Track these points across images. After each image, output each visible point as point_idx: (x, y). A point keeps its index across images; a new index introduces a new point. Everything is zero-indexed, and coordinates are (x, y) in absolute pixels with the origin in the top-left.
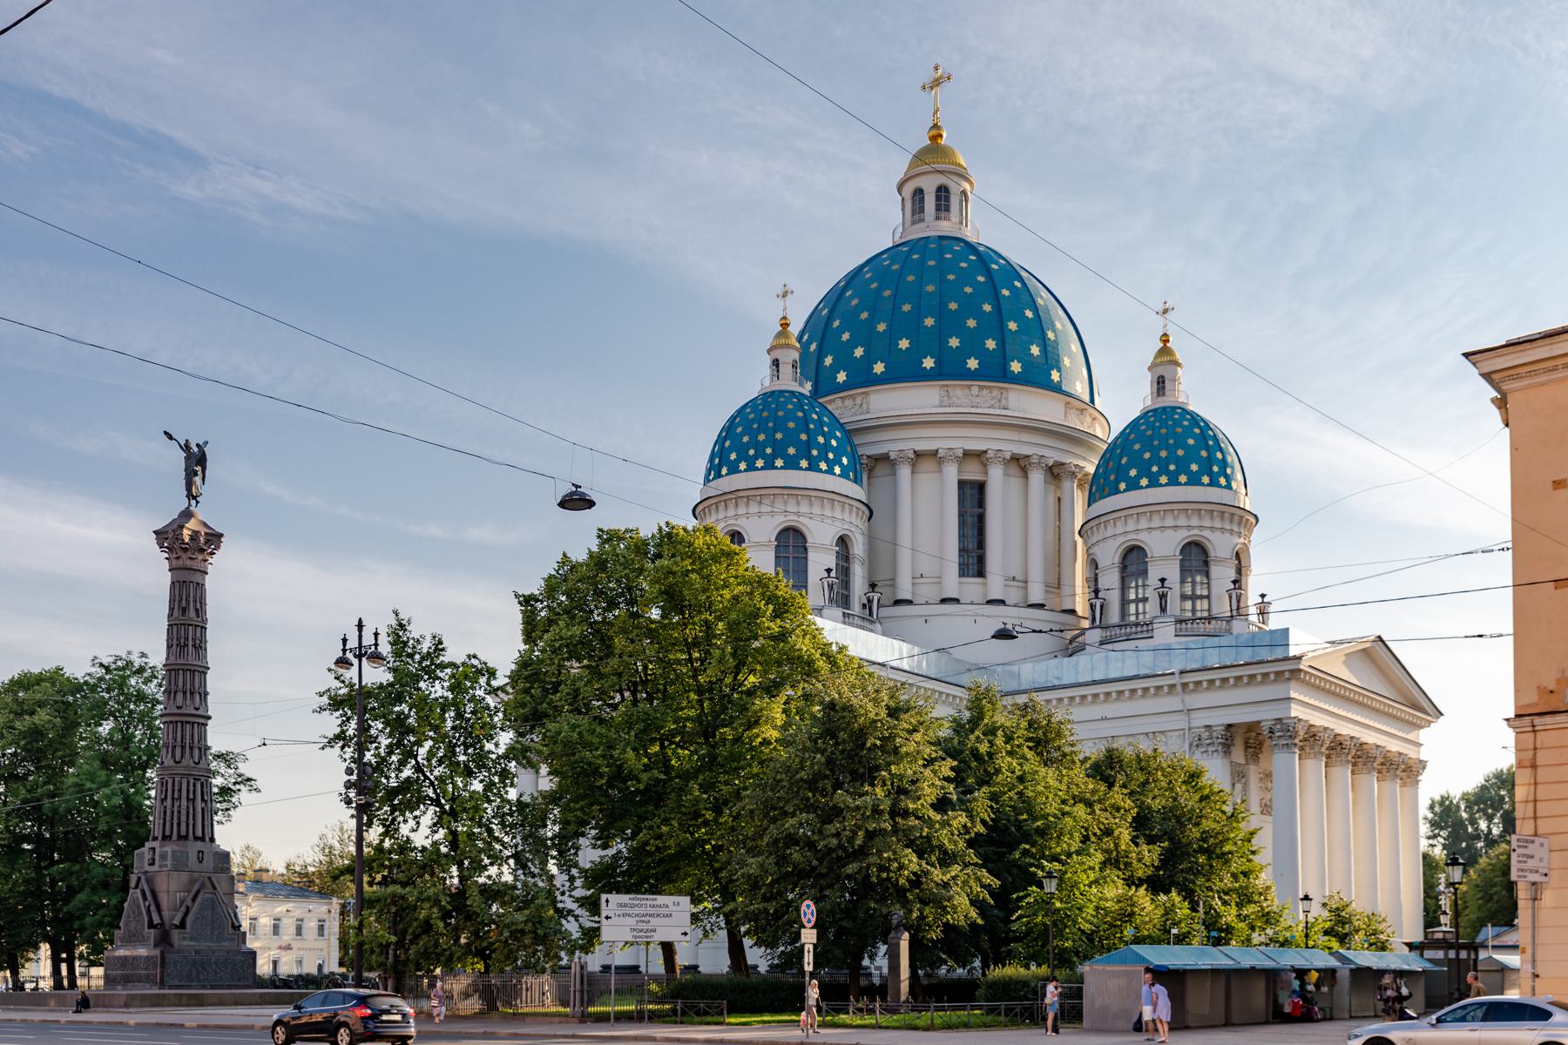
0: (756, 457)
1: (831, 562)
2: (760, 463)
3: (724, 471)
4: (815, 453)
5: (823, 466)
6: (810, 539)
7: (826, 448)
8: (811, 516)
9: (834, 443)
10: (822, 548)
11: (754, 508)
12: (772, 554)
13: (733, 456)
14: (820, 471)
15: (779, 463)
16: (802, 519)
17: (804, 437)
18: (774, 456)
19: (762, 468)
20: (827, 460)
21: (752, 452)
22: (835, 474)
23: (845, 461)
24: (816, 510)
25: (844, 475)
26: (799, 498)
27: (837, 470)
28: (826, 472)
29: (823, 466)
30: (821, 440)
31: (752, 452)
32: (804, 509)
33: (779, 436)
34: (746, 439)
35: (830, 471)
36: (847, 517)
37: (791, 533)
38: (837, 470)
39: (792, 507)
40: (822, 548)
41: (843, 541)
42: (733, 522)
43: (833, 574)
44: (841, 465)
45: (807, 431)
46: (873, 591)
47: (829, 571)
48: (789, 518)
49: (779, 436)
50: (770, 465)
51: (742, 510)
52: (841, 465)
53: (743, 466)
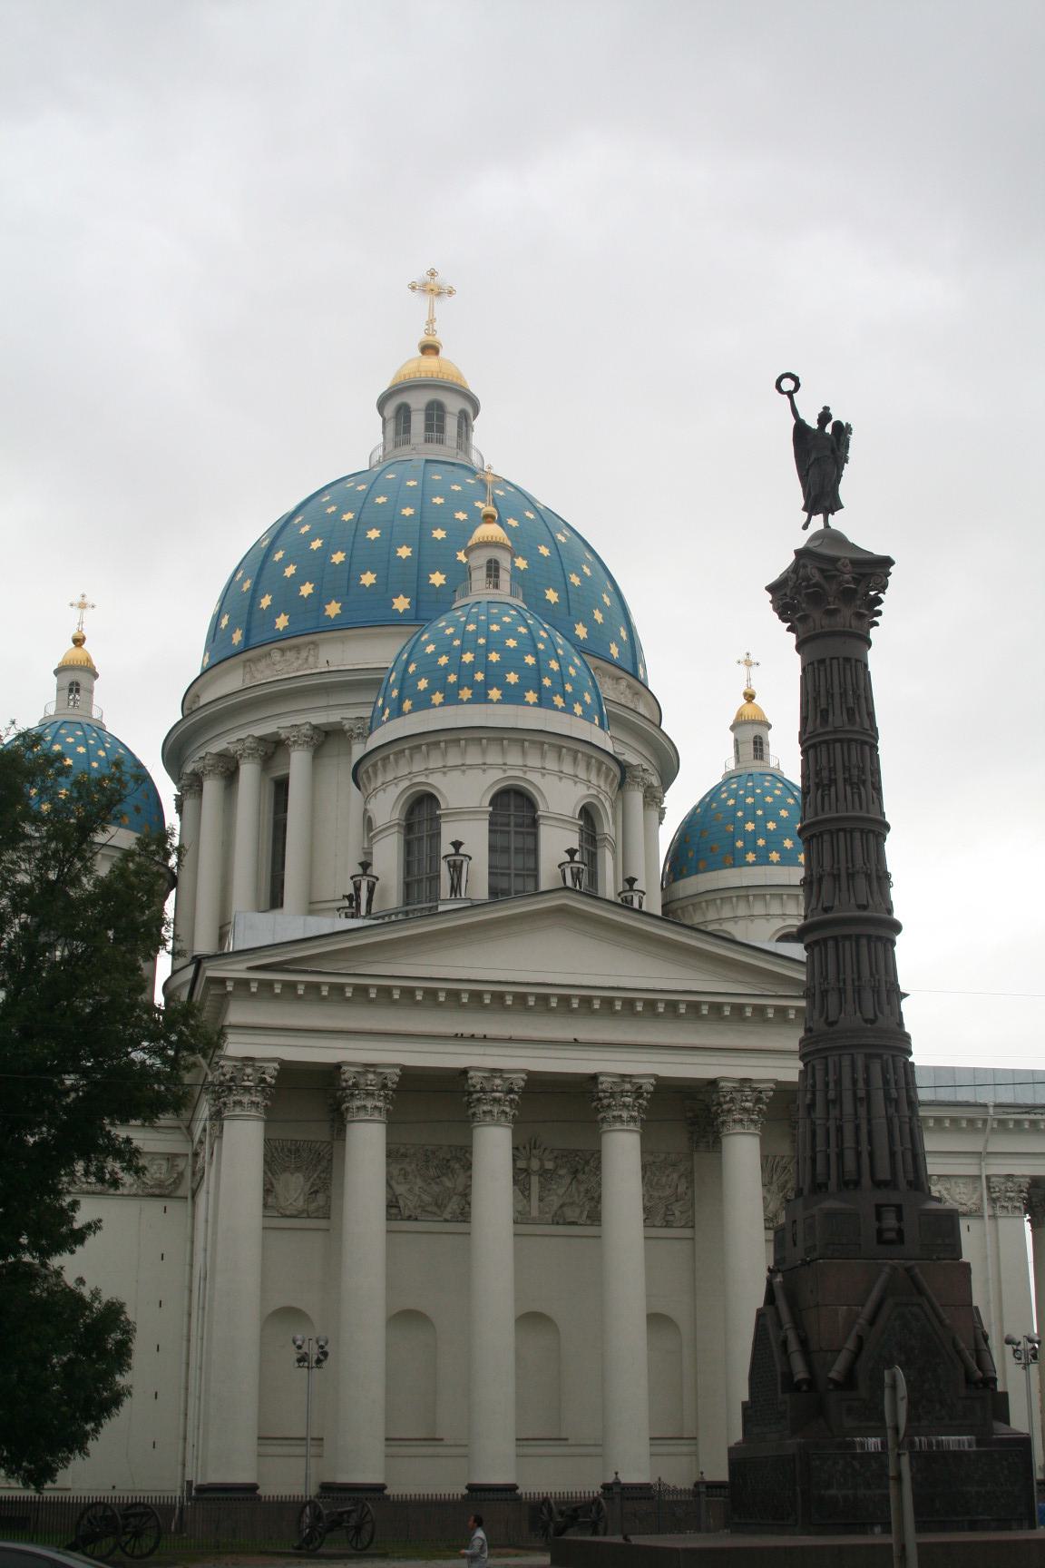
1: (573, 840)
2: (466, 694)
3: (407, 705)
4: (547, 682)
5: (558, 701)
6: (541, 806)
7: (561, 677)
8: (543, 771)
9: (572, 671)
10: (560, 820)
11: (454, 758)
12: (485, 825)
13: (423, 684)
14: (555, 708)
15: (495, 694)
16: (531, 776)
17: (530, 660)
18: (487, 685)
19: (469, 702)
20: (564, 695)
21: (452, 678)
22: (575, 714)
23: (587, 698)
24: (551, 764)
25: (587, 716)
27: (578, 709)
28: (563, 710)
29: (558, 701)
30: (554, 665)
32: (534, 761)
33: (494, 657)
34: (443, 660)
35: (568, 710)
37: (512, 794)
38: (578, 709)
39: (514, 758)
40: (560, 820)
41: (588, 814)
43: (577, 858)
44: (583, 703)
46: (631, 889)
47: (571, 852)
48: (510, 773)
49: (494, 657)
50: (481, 697)
51: (436, 761)
52: (583, 703)
53: (438, 698)
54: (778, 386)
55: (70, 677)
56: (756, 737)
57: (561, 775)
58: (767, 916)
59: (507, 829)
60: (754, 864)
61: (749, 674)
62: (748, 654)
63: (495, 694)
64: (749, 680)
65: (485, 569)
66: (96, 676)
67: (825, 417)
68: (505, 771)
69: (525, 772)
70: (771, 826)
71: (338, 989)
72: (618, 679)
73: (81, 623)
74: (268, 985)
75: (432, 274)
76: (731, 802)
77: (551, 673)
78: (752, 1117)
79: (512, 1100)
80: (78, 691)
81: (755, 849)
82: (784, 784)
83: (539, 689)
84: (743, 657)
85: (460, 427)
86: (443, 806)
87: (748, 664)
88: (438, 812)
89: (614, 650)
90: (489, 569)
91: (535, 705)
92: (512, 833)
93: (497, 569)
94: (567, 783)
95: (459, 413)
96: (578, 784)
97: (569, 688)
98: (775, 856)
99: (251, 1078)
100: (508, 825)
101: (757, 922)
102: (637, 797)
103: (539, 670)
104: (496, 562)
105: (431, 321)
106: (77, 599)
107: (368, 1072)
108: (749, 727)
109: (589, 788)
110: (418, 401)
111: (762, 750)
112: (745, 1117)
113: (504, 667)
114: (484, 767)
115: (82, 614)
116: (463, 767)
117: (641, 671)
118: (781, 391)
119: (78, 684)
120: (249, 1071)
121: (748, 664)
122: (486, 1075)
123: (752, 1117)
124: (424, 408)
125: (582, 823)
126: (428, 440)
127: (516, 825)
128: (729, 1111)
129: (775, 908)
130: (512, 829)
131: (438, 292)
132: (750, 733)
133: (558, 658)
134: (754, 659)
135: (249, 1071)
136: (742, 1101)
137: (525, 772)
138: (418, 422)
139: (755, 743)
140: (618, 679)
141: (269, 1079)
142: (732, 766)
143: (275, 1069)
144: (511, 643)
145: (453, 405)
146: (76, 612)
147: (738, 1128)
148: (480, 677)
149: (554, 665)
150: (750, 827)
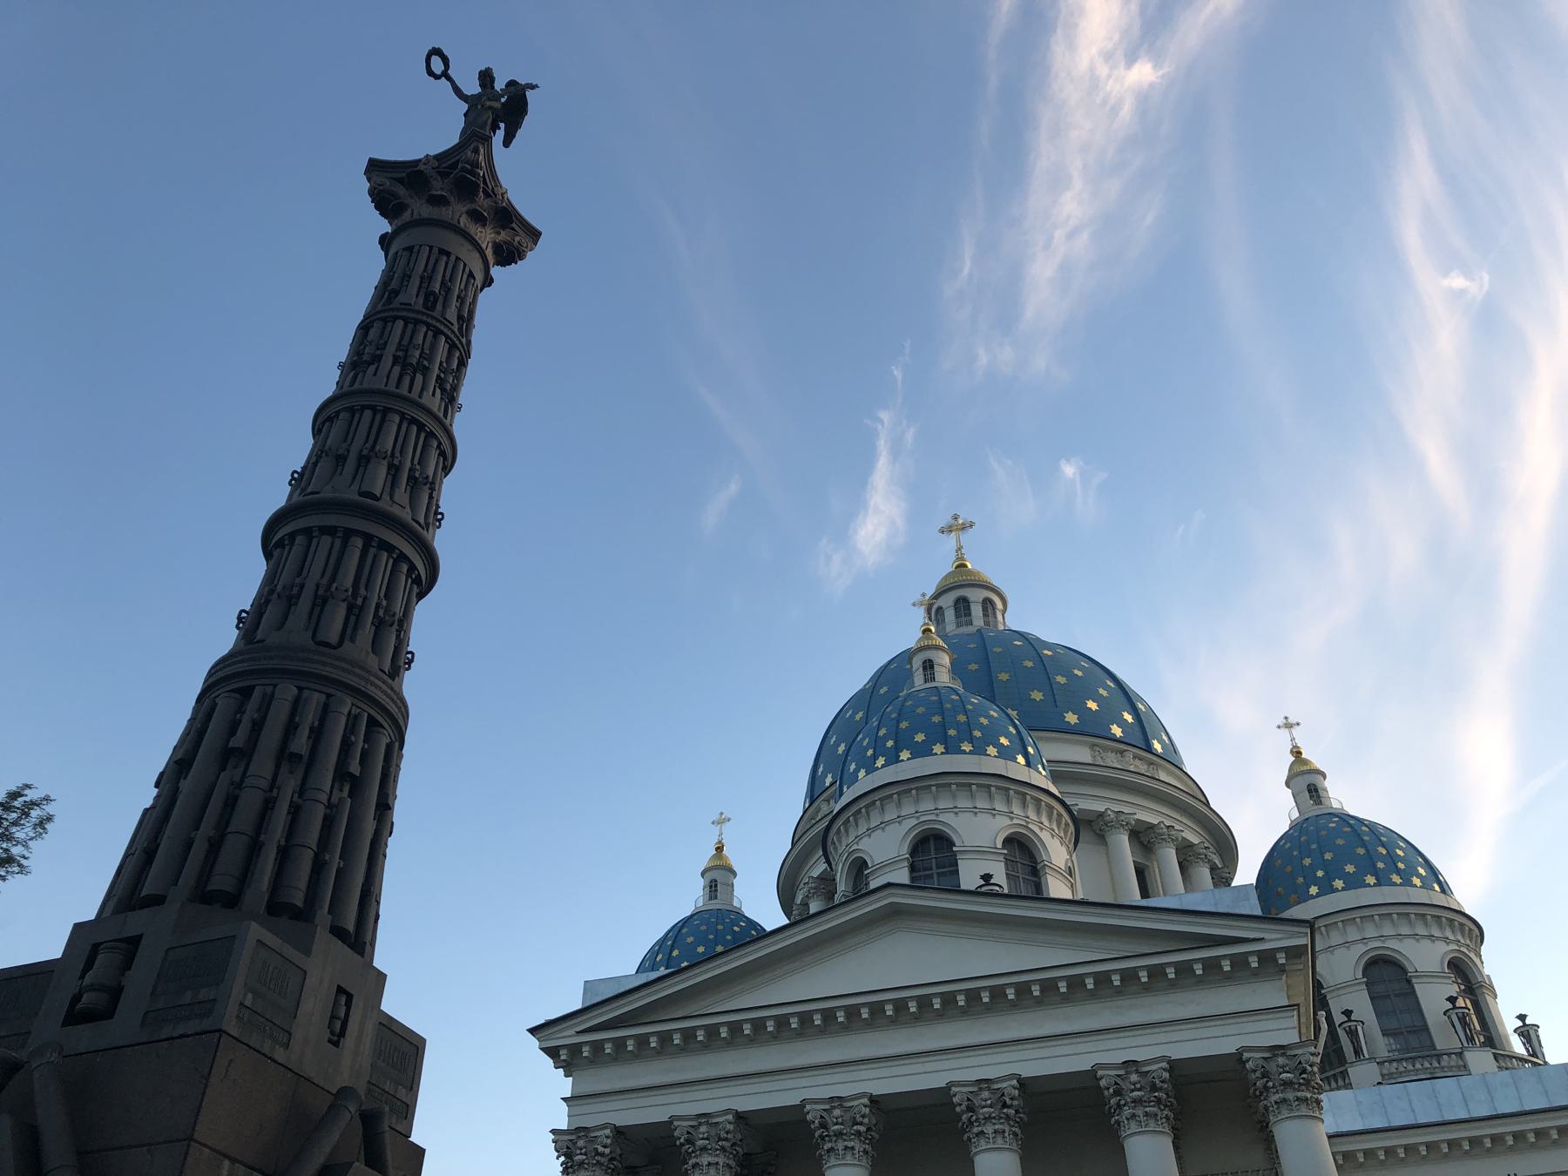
0: (875, 757)
2: (880, 762)
4: (952, 732)
5: (967, 747)
8: (956, 811)
10: (979, 852)
13: (853, 766)
14: (964, 752)
18: (897, 750)
20: (971, 740)
24: (963, 803)
26: (934, 788)
27: (992, 750)
28: (971, 753)
30: (962, 718)
31: (870, 752)
32: (943, 804)
33: (904, 725)
36: (1017, 810)
39: (926, 805)
40: (979, 852)
42: (855, 847)
45: (942, 713)
48: (922, 819)
51: (862, 829)
54: (430, 73)
55: (710, 875)
56: (1309, 786)
57: (975, 811)
58: (1347, 944)
59: (929, 872)
60: (1318, 895)
61: (1291, 733)
62: (1286, 718)
63: (905, 755)
64: (1293, 739)
65: (921, 669)
66: (734, 874)
67: (486, 77)
68: (918, 818)
69: (937, 815)
70: (1328, 856)
71: (665, 1038)
72: (1122, 752)
73: (721, 834)
74: (597, 1047)
75: (956, 518)
76: (1288, 845)
77: (958, 726)
78: (1148, 1109)
79: (859, 1133)
80: (716, 886)
81: (1317, 881)
82: (1339, 817)
83: (945, 740)
84: (1281, 721)
85: (985, 610)
86: (870, 866)
87: (1289, 726)
88: (866, 872)
89: (1117, 731)
90: (925, 669)
91: (942, 753)
92: (935, 876)
93: (932, 667)
94: (984, 818)
95: (983, 601)
96: (997, 816)
97: (977, 734)
98: (1339, 884)
99: (583, 1151)
100: (931, 869)
101: (1338, 952)
102: (1170, 855)
103: (944, 726)
104: (930, 661)
105: (959, 549)
106: (716, 817)
107: (700, 1124)
108: (1300, 778)
109: (1012, 819)
110: (947, 601)
111: (1319, 797)
112: (1139, 1112)
113: (914, 730)
114: (900, 819)
115: (721, 828)
116: (883, 825)
117: (1157, 746)
118: (437, 77)
119: (716, 881)
120: (581, 1143)
121: (1289, 726)
122: (827, 1107)
123: (1148, 1109)
124: (953, 604)
125: (1006, 852)
126: (959, 625)
127: (937, 868)
128: (1119, 1106)
129: (1353, 934)
130: (935, 871)
131: (964, 528)
132: (1302, 782)
133: (965, 712)
134: (1292, 720)
135: (581, 1143)
136: (1133, 1091)
137: (937, 815)
138: (950, 615)
139: (1310, 791)
140: (1122, 752)
141: (601, 1149)
142: (1296, 814)
143: (607, 1137)
144: (920, 710)
145: (976, 596)
146: (716, 829)
147: (1134, 1127)
148: (890, 744)
149: (962, 718)
150: (1307, 861)
